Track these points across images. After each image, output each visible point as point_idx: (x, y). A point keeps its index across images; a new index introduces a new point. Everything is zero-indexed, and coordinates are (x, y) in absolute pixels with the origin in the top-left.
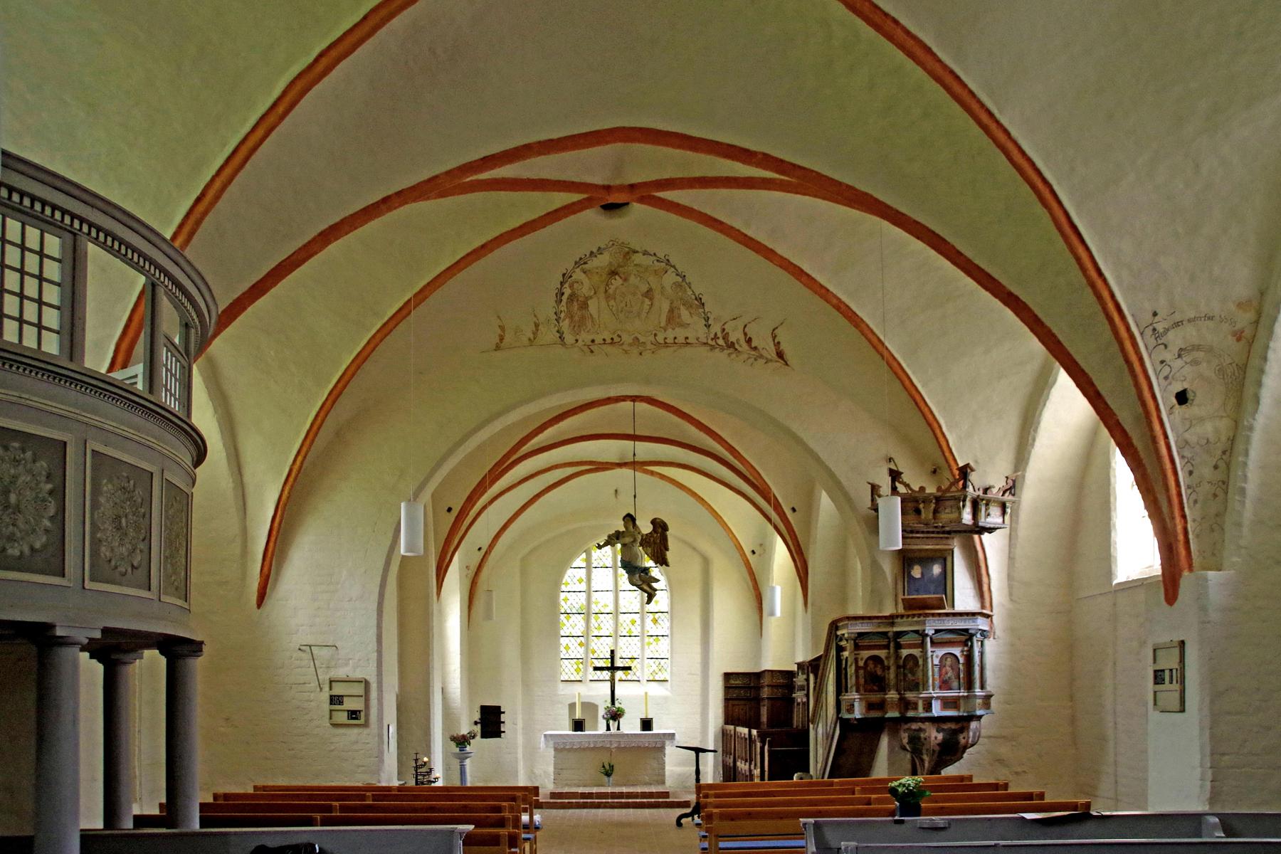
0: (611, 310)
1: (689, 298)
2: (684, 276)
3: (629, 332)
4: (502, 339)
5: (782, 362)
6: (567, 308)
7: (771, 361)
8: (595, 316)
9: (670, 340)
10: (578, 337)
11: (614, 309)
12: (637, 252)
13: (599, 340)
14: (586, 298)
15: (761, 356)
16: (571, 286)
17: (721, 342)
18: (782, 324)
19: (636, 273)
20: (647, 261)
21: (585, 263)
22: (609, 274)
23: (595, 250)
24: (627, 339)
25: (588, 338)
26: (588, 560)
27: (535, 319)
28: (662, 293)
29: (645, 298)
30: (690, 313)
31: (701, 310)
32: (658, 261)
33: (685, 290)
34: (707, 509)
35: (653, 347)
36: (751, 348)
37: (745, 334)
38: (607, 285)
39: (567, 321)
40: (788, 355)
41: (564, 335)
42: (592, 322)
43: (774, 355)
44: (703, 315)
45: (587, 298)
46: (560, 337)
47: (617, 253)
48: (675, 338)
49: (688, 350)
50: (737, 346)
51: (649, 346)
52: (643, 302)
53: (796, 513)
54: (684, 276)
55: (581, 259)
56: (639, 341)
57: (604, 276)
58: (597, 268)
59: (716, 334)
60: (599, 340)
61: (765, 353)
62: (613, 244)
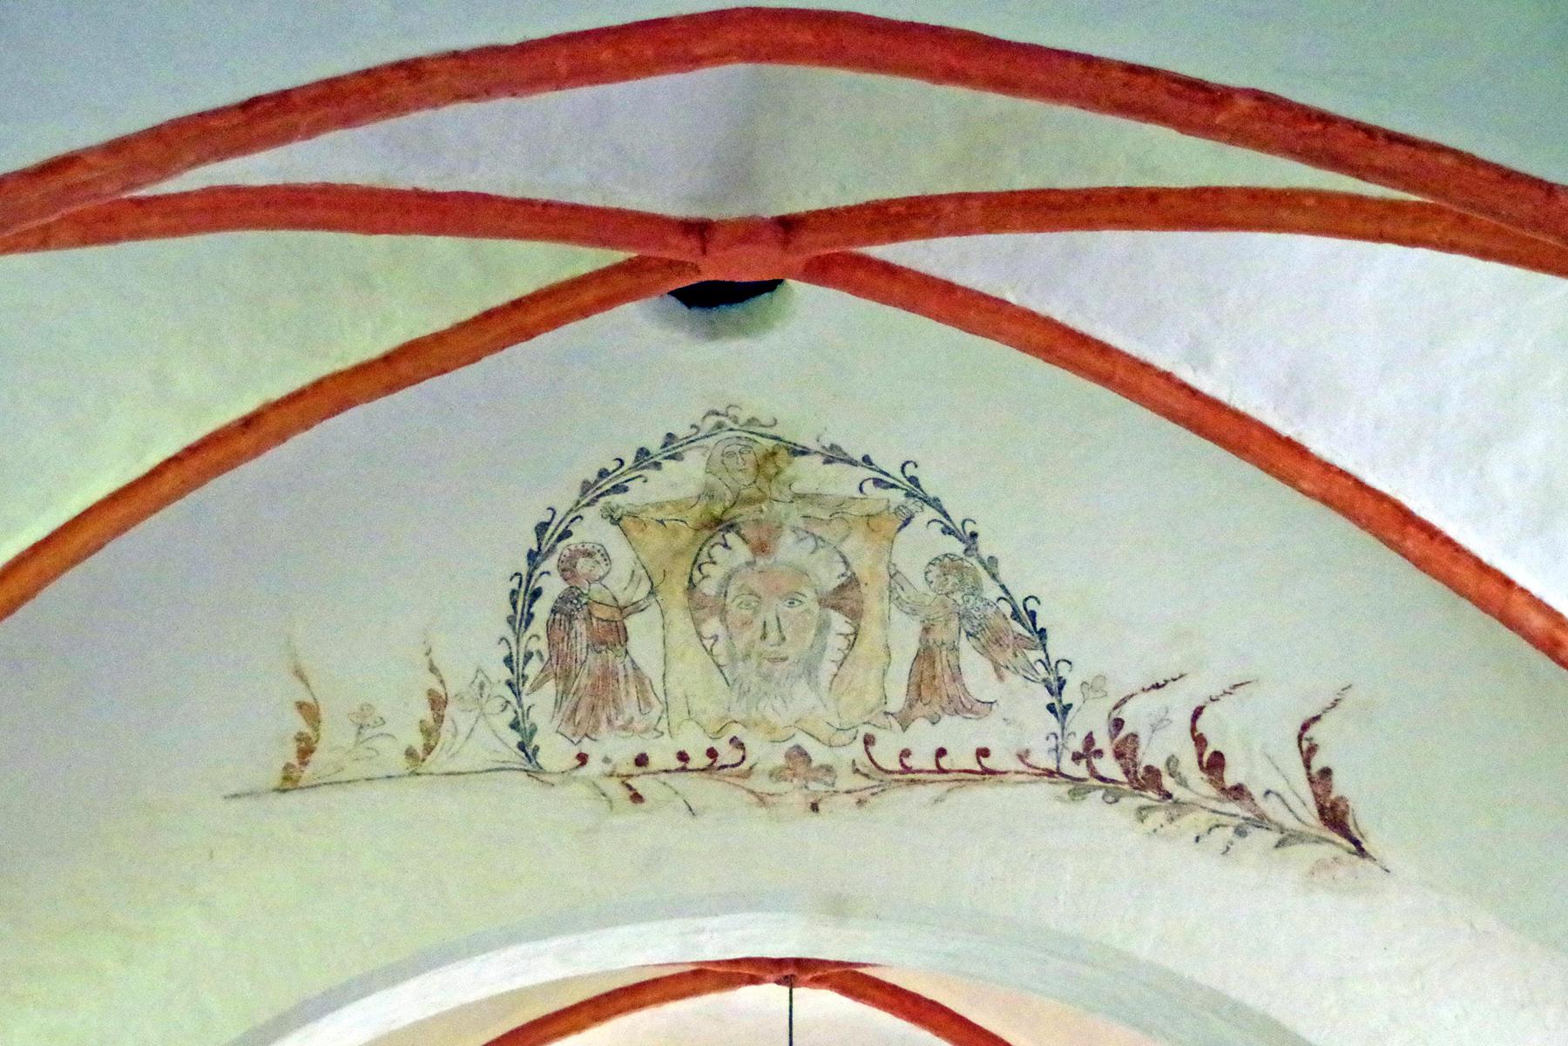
0: (710, 652)
1: (990, 611)
2: (974, 535)
4: (306, 751)
5: (1344, 842)
6: (551, 645)
8: (652, 669)
9: (922, 759)
10: (587, 746)
11: (719, 649)
12: (805, 452)
13: (662, 756)
14: (621, 609)
15: (1261, 821)
16: (567, 570)
17: (1109, 766)
18: (1334, 705)
19: (801, 523)
20: (842, 482)
21: (619, 489)
23: (654, 445)
24: (765, 753)
27: (432, 682)
32: (877, 482)
33: (976, 589)
35: (861, 782)
37: (1200, 741)
38: (697, 564)
39: (550, 688)
40: (1363, 818)
41: (536, 740)
43: (1310, 814)
45: (625, 610)
46: (522, 746)
47: (731, 454)
48: (941, 752)
49: (985, 793)
50: (1168, 783)
51: (846, 780)
52: (823, 627)
54: (974, 535)
55: (603, 474)
56: (810, 761)
57: (686, 535)
58: (660, 506)
59: (1089, 739)
60: (662, 756)
61: (1271, 808)
62: (719, 426)
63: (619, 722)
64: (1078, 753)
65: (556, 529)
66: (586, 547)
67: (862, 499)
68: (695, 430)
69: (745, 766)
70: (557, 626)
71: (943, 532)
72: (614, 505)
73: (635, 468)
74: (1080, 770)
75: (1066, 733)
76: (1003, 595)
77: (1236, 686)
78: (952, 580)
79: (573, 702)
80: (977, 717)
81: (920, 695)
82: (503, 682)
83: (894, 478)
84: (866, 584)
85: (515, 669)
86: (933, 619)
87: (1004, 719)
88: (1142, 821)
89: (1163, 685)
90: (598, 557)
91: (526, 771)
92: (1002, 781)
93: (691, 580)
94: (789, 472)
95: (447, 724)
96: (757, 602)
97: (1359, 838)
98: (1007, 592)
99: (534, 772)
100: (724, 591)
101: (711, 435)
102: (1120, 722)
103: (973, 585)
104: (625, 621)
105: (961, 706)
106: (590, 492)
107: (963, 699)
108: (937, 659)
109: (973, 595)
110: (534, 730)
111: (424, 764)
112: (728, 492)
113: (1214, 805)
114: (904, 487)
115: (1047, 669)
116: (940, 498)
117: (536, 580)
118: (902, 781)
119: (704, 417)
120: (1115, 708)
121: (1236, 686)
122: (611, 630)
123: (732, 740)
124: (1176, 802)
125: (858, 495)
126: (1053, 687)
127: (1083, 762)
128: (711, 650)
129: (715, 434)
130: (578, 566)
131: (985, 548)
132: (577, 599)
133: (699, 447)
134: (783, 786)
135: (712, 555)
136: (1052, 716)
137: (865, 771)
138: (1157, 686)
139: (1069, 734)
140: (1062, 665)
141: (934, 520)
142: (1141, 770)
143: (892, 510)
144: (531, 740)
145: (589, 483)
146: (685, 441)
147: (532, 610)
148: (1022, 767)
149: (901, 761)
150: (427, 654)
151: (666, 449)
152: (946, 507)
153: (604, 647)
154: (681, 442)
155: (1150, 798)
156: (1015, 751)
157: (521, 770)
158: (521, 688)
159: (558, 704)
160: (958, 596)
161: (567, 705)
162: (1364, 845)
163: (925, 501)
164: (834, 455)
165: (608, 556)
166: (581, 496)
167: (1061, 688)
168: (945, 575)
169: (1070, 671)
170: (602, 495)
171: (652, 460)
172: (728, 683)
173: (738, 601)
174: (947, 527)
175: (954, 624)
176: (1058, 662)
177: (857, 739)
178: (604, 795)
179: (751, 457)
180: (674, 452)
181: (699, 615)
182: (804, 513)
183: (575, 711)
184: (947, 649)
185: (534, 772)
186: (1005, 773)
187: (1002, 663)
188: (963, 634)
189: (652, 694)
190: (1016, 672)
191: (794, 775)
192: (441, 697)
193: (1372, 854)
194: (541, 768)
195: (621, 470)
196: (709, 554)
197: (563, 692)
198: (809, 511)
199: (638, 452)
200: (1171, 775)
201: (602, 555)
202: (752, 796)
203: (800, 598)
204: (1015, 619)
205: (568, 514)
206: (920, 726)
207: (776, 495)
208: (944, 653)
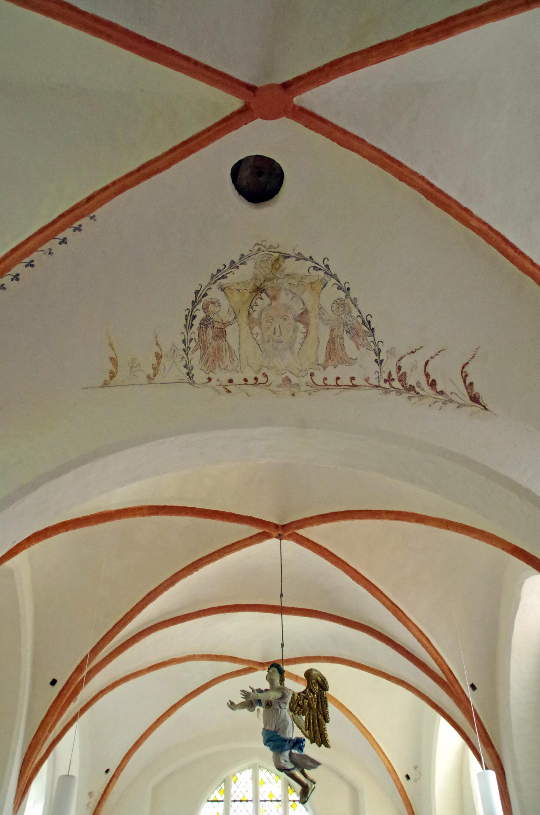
2: (349, 289)
3: (278, 370)
4: (112, 375)
7: (465, 405)
9: (331, 381)
10: (211, 375)
11: (258, 338)
13: (238, 379)
14: (224, 324)
15: (451, 401)
16: (205, 309)
17: (396, 384)
18: (473, 357)
19: (288, 287)
21: (224, 277)
22: (254, 291)
23: (236, 260)
24: (275, 379)
25: (224, 377)
26: (227, 792)
27: (157, 349)
28: (321, 318)
29: (298, 323)
30: (357, 343)
31: (371, 339)
32: (314, 268)
33: (350, 311)
34: (355, 724)
35: (309, 388)
36: (437, 392)
37: (427, 375)
38: (251, 306)
39: (198, 353)
40: (484, 399)
41: (193, 372)
42: (231, 356)
44: (373, 347)
46: (188, 374)
48: (338, 378)
49: (353, 392)
50: (417, 389)
52: (296, 329)
53: (476, 691)
55: (219, 271)
56: (291, 382)
57: (247, 295)
58: (238, 284)
59: (390, 374)
60: (238, 379)
61: (453, 397)
63: (223, 367)
64: (386, 379)
65: (202, 293)
66: (212, 300)
67: (309, 276)
68: (251, 252)
69: (268, 383)
70: (201, 329)
71: (338, 289)
72: (222, 284)
73: (229, 268)
74: (387, 385)
75: (382, 371)
76: (359, 315)
77: (439, 352)
78: (341, 309)
79: (207, 358)
80: (350, 365)
81: (330, 357)
82: (182, 349)
83: (321, 266)
84: (311, 312)
85: (186, 344)
86: (334, 326)
87: (360, 366)
88: (410, 400)
89: (415, 352)
90: (216, 304)
91: (189, 383)
92: (360, 389)
93: (249, 313)
94: (284, 265)
95: (162, 366)
96: (272, 320)
97: (484, 405)
98: (360, 313)
99: (192, 383)
100: (260, 316)
101: (256, 254)
102: (400, 367)
103: (349, 310)
104: (225, 328)
105: (345, 361)
106: (214, 278)
107: (345, 358)
108: (336, 342)
109: (348, 315)
110: (192, 368)
111: (154, 380)
112: (262, 277)
113: (435, 396)
114: (324, 270)
115: (374, 345)
116: (337, 274)
117: (194, 312)
118: (324, 388)
119: (254, 246)
120: (399, 361)
121: (439, 352)
122: (220, 331)
123: (264, 374)
124: (421, 395)
125: (307, 273)
126: (377, 353)
127: (388, 383)
128: (256, 339)
129: (258, 253)
130: (209, 308)
131: (352, 296)
132: (208, 320)
133: (252, 259)
134: (281, 389)
135: (256, 302)
136: (376, 364)
137: (311, 385)
138: (413, 352)
139: (383, 372)
140: (380, 343)
141: (334, 284)
142: (408, 386)
143: (320, 281)
144: (191, 372)
145: (214, 275)
146: (247, 257)
147: (193, 323)
148: (367, 384)
149: (324, 382)
150: (156, 338)
151: (241, 260)
152: (339, 278)
153: (218, 338)
154: (246, 257)
155: (412, 394)
156: (364, 378)
157: (187, 383)
158: (188, 352)
159: (201, 359)
160: (343, 316)
161: (205, 359)
162: (487, 407)
163: (331, 276)
164: (300, 257)
165: (220, 304)
166: (211, 280)
167: (379, 353)
168: (338, 307)
169: (383, 346)
170: (218, 279)
171: (236, 265)
172: (262, 351)
173: (265, 320)
174: (339, 286)
175: (342, 328)
176: (378, 342)
177: (308, 374)
178: (217, 391)
179: (270, 261)
180: (243, 261)
181: (251, 325)
182: (288, 282)
183: (207, 362)
184: (339, 338)
185: (192, 383)
186: (361, 386)
187: (359, 343)
188: (345, 331)
189: (235, 357)
190: (364, 346)
191: (286, 386)
192: (160, 355)
193: (489, 409)
194: (195, 382)
195: (225, 269)
196: (255, 302)
197: (203, 354)
198: (290, 281)
199: (231, 262)
200: (419, 387)
201: (218, 303)
202: (270, 391)
203: (287, 318)
204: (363, 324)
205: (206, 287)
206: (330, 369)
207: (279, 275)
208: (338, 340)
